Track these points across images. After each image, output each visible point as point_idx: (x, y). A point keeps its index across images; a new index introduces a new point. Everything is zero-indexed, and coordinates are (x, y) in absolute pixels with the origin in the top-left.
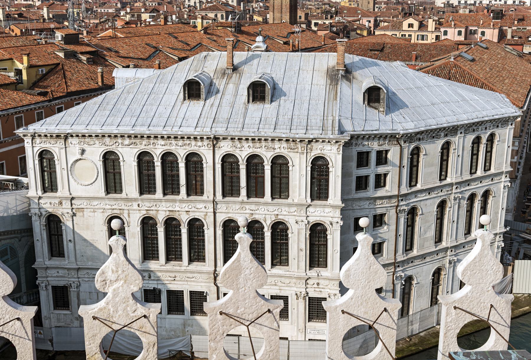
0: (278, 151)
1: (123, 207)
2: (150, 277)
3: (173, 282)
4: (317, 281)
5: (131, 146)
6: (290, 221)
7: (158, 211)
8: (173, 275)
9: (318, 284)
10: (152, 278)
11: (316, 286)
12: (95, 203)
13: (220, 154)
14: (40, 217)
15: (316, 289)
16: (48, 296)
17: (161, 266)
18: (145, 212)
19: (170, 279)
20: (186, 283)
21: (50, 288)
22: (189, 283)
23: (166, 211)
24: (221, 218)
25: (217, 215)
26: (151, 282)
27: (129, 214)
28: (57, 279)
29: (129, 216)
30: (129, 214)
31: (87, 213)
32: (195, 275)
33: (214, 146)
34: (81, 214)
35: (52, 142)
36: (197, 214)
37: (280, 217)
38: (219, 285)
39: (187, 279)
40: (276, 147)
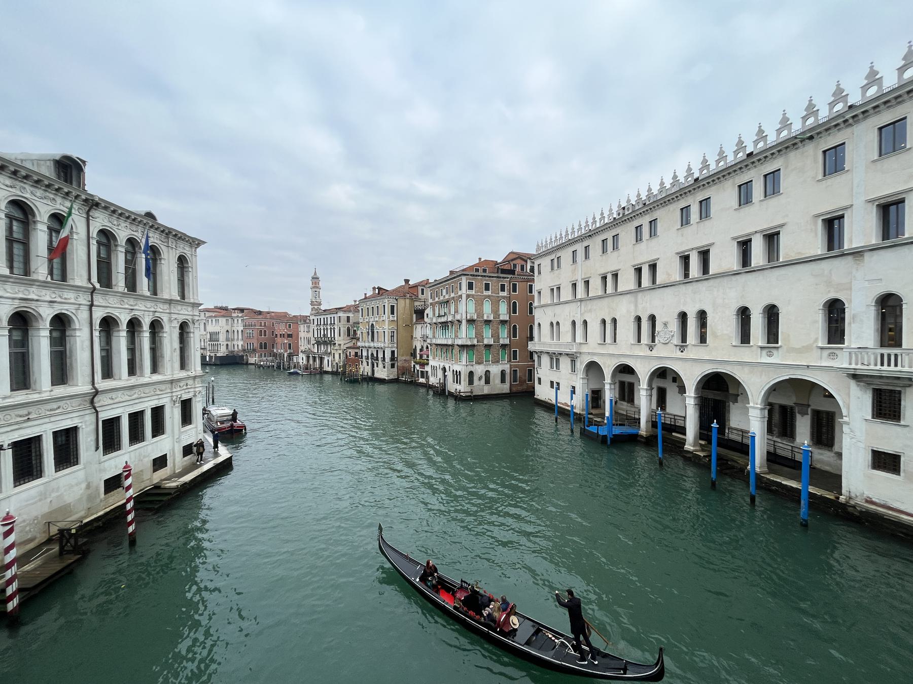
6: (165, 319)
8: (23, 411)
20: (47, 420)
22: (53, 419)
23: (13, 299)
24: (98, 314)
32: (61, 404)
33: (88, 213)
36: (66, 307)
37: (157, 314)
38: (98, 409)
39: (48, 413)
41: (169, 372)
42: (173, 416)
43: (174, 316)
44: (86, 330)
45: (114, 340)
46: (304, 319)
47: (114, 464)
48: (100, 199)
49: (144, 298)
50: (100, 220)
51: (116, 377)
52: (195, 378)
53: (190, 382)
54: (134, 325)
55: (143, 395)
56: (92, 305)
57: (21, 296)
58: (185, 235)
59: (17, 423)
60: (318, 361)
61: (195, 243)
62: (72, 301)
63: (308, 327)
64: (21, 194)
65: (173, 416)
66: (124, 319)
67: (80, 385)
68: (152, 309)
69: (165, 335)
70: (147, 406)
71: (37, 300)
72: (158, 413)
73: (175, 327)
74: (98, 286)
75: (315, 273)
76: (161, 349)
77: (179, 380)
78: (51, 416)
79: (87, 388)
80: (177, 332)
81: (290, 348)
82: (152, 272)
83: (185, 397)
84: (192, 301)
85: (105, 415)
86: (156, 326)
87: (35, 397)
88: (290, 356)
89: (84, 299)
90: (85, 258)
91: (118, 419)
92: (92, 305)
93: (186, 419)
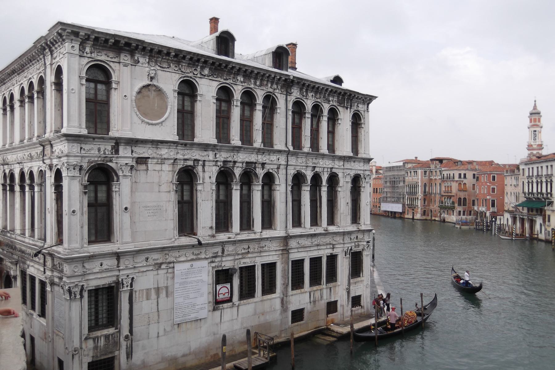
1: (197, 157)
2: (223, 252)
5: (210, 78)
7: (235, 162)
10: (226, 253)
12: (164, 152)
13: (292, 99)
14: (81, 168)
15: (356, 244)
17: (237, 234)
19: (243, 251)
20: (258, 254)
21: (86, 295)
23: (243, 163)
24: (292, 172)
26: (224, 259)
28: (99, 276)
29: (204, 171)
30: (204, 166)
34: (143, 167)
35: (111, 55)
36: (272, 167)
37: (334, 170)
40: (331, 99)
41: (343, 223)
42: (343, 266)
43: (348, 172)
44: (283, 186)
45: (303, 192)
46: (514, 169)
47: (300, 299)
48: (294, 77)
49: (323, 156)
50: (296, 94)
51: (303, 226)
52: (364, 231)
53: (360, 236)
54: (316, 178)
55: (321, 243)
56: (287, 165)
57: (247, 160)
58: (358, 93)
59: (243, 254)
60: (527, 225)
61: (368, 99)
62: (275, 162)
63: (517, 179)
64: (248, 86)
65: (343, 266)
66: (309, 175)
67: (279, 231)
68: (331, 166)
69: (339, 189)
70: (324, 253)
71: (256, 163)
73: (347, 182)
74: (291, 148)
75: (535, 107)
76: (336, 202)
77: (350, 233)
78: (261, 252)
79: (282, 234)
80: (350, 185)
81: (493, 205)
82: (332, 133)
83: (355, 249)
84: (364, 156)
85: (295, 256)
86: (333, 179)
87: (252, 236)
88: (494, 215)
89: (283, 161)
90: (284, 127)
91: (302, 261)
92: (287, 165)
93: (356, 270)
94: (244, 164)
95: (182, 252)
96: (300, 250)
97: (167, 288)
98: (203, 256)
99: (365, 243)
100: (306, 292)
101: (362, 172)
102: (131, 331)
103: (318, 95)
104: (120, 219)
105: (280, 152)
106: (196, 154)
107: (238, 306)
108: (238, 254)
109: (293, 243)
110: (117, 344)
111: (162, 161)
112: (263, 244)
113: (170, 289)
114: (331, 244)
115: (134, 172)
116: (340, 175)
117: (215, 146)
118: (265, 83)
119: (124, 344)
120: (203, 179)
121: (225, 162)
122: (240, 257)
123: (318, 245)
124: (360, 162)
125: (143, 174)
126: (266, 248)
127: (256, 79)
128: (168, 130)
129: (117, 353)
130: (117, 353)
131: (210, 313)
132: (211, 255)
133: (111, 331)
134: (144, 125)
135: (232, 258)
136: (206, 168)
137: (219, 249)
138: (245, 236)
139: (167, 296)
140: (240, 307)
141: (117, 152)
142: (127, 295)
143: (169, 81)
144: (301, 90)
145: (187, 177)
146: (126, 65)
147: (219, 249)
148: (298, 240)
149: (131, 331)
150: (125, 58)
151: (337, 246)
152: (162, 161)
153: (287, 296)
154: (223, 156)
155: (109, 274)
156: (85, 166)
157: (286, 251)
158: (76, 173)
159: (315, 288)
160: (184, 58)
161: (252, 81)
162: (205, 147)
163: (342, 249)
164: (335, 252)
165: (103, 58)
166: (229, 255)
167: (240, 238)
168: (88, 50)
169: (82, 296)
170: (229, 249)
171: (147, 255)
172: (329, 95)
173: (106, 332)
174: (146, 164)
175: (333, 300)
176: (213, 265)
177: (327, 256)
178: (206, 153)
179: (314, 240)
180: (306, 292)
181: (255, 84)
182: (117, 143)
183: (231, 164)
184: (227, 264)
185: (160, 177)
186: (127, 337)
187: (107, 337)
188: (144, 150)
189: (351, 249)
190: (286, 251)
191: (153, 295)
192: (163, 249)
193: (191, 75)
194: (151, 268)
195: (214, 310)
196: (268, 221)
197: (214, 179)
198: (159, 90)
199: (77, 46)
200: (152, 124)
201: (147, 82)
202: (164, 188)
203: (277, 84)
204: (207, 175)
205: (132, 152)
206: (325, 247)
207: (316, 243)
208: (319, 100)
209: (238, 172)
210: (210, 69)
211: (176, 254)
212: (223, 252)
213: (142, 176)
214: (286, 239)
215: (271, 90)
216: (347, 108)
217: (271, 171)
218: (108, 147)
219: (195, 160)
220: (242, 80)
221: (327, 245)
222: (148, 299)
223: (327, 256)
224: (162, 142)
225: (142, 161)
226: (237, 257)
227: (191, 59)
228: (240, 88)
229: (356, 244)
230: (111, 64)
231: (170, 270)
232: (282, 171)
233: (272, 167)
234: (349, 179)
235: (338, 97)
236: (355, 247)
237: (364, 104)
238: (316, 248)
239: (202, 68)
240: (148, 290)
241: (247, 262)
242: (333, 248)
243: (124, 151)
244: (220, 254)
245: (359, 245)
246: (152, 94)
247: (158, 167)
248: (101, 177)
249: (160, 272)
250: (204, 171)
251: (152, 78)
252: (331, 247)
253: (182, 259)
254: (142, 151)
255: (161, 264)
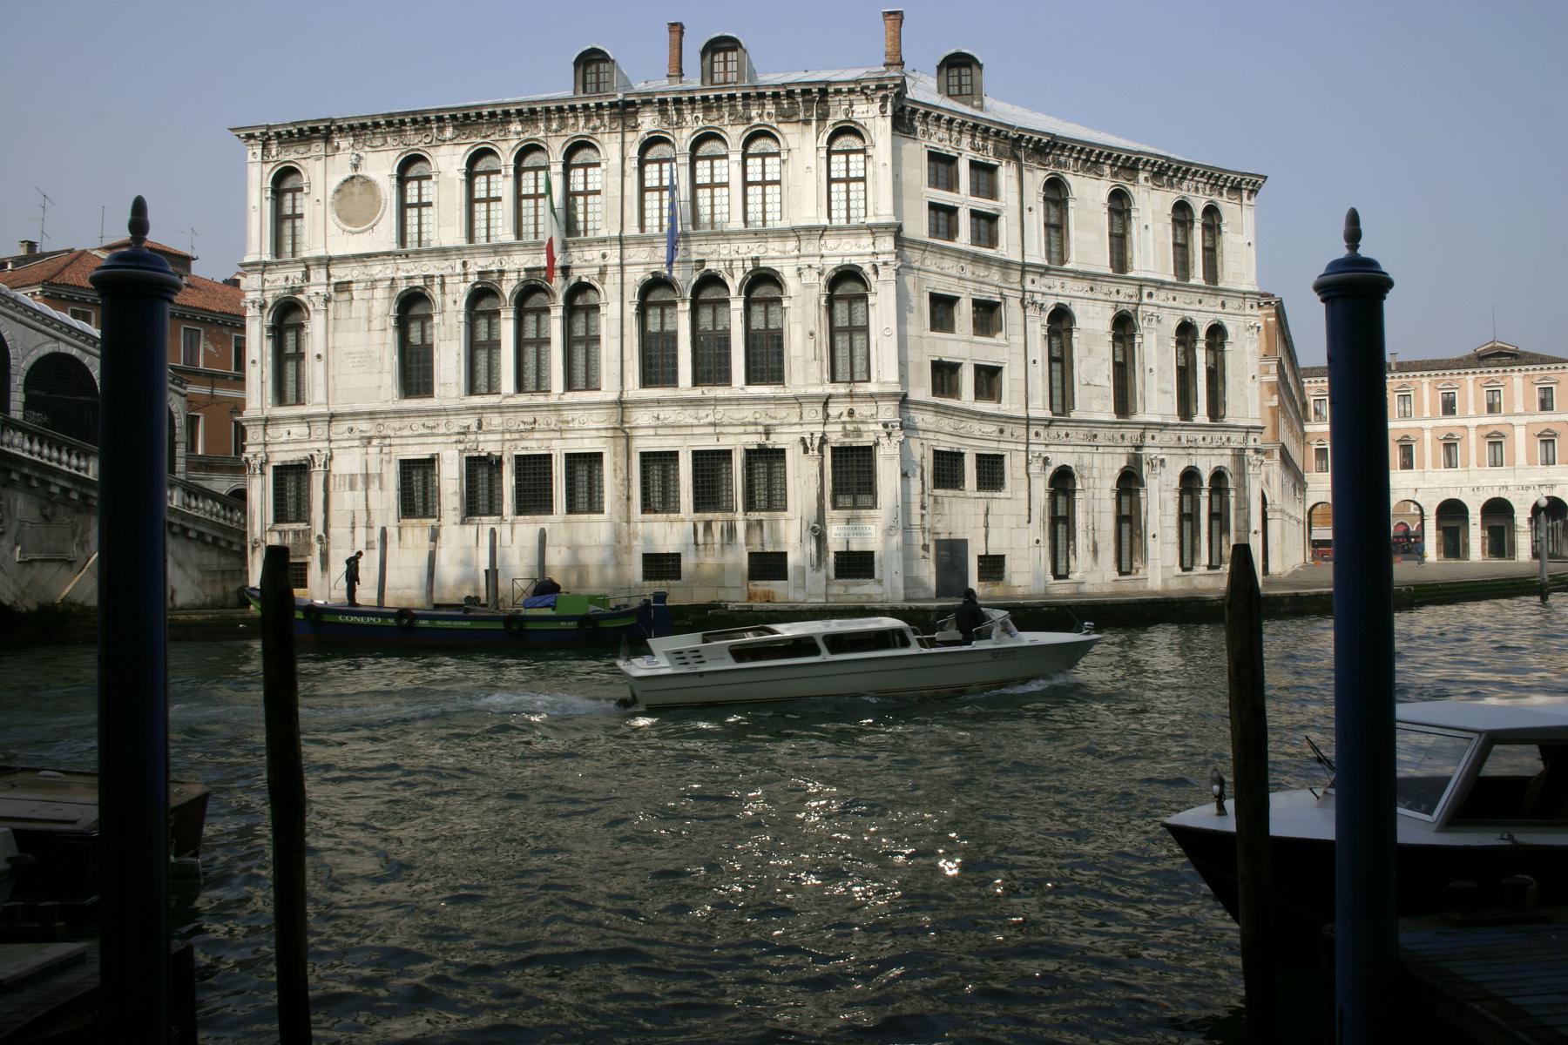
0: (757, 121)
2: (480, 426)
3: (531, 435)
4: (850, 406)
7: (501, 272)
8: (529, 417)
9: (851, 413)
11: (845, 418)
14: (262, 307)
15: (849, 427)
16: (264, 489)
18: (473, 279)
20: (558, 435)
21: (270, 472)
24: (636, 276)
25: (628, 269)
26: (481, 438)
27: (443, 285)
28: (285, 447)
29: (443, 292)
30: (443, 285)
31: (357, 291)
34: (346, 296)
35: (302, 149)
36: (586, 271)
37: (762, 264)
40: (754, 113)
42: (804, 479)
53: (863, 409)
55: (726, 420)
56: (622, 265)
57: (530, 265)
65: (804, 479)
68: (754, 254)
70: (738, 442)
72: (766, 460)
73: (809, 286)
77: (826, 401)
79: (614, 396)
85: (647, 442)
94: (523, 274)
95: (407, 422)
96: (660, 431)
97: (380, 476)
98: (442, 430)
99: (880, 427)
100: (683, 520)
101: (867, 259)
102: (326, 530)
103: (714, 114)
104: (314, 372)
105: (603, 241)
106: (432, 266)
107: (512, 524)
108: (510, 432)
109: (641, 417)
110: (309, 545)
111: (373, 284)
112: (568, 415)
113: (385, 477)
114: (756, 424)
115: (331, 305)
116: (788, 273)
117: (458, 249)
118: (571, 121)
119: (317, 548)
120: (443, 305)
121: (480, 273)
122: (516, 436)
123: (714, 425)
124: (859, 236)
125: (344, 307)
126: (576, 425)
127: (549, 120)
128: (383, 236)
129: (309, 559)
130: (309, 559)
131: (457, 528)
132: (457, 429)
133: (302, 526)
134: (346, 235)
135: (498, 437)
136: (447, 289)
137: (472, 421)
138: (523, 399)
139: (381, 488)
140: (517, 527)
141: (308, 278)
142: (322, 478)
143: (381, 164)
144: (663, 113)
145: (412, 306)
146: (318, 159)
147: (472, 421)
148: (656, 411)
149: (326, 530)
150: (318, 148)
151: (779, 429)
152: (373, 284)
153: (628, 522)
154: (478, 263)
155: (298, 446)
156: (270, 303)
157: (623, 432)
158: (256, 312)
159: (709, 516)
160: (403, 123)
161: (541, 125)
162: (443, 252)
163: (798, 437)
164: (776, 441)
165: (292, 156)
166: (489, 432)
167: (511, 401)
168: (274, 152)
169: (263, 473)
170: (495, 420)
171: (350, 424)
172: (746, 106)
173: (295, 526)
174: (350, 291)
175: (769, 549)
176: (461, 447)
177: (748, 452)
178: (447, 263)
179: (702, 413)
180: (683, 520)
181: (548, 129)
182: (307, 264)
183: (495, 276)
184: (489, 445)
185: (369, 309)
186: (320, 538)
187: (296, 533)
188: (348, 271)
189: (823, 441)
190: (623, 432)
191: (360, 484)
192: (372, 415)
193: (421, 145)
194: (357, 443)
195: (463, 522)
196: (581, 375)
197: (462, 305)
198: (368, 183)
199: (258, 150)
200: (353, 233)
201: (349, 173)
202: (377, 324)
203: (600, 117)
204: (449, 300)
205: (329, 276)
206: (741, 429)
207: (711, 419)
208: (716, 124)
209: (508, 288)
210: (455, 127)
211: (396, 424)
212: (480, 426)
213: (340, 308)
214: (621, 404)
215: (586, 132)
216: (807, 122)
217: (585, 280)
218: (296, 274)
219: (425, 277)
220: (519, 128)
221: (744, 424)
222: (352, 487)
223: (748, 452)
224: (369, 256)
225: (343, 287)
226: (507, 436)
227: (414, 121)
228: (513, 143)
229: (849, 427)
230: (303, 162)
231: (386, 450)
232: (613, 277)
233: (586, 271)
234: (811, 277)
235: (778, 104)
236: (846, 435)
237: (870, 99)
238: (711, 430)
239: (441, 130)
240: (353, 477)
241: (533, 447)
242: (767, 433)
243: (318, 275)
244: (474, 428)
245: (858, 433)
246: (357, 188)
247: (368, 294)
248: (287, 316)
249: (370, 450)
250: (443, 292)
251: (356, 167)
252: (761, 429)
253: (406, 432)
254: (340, 273)
255: (370, 439)
